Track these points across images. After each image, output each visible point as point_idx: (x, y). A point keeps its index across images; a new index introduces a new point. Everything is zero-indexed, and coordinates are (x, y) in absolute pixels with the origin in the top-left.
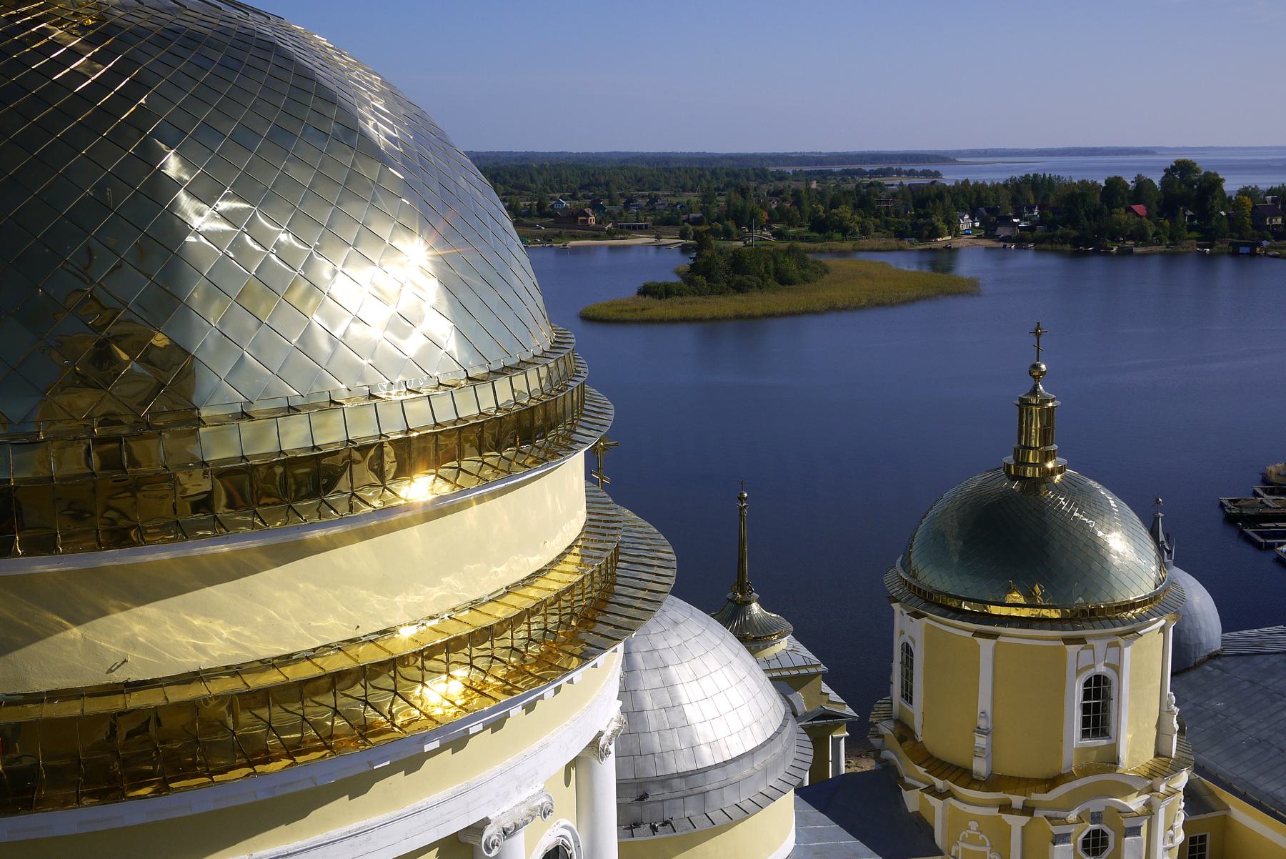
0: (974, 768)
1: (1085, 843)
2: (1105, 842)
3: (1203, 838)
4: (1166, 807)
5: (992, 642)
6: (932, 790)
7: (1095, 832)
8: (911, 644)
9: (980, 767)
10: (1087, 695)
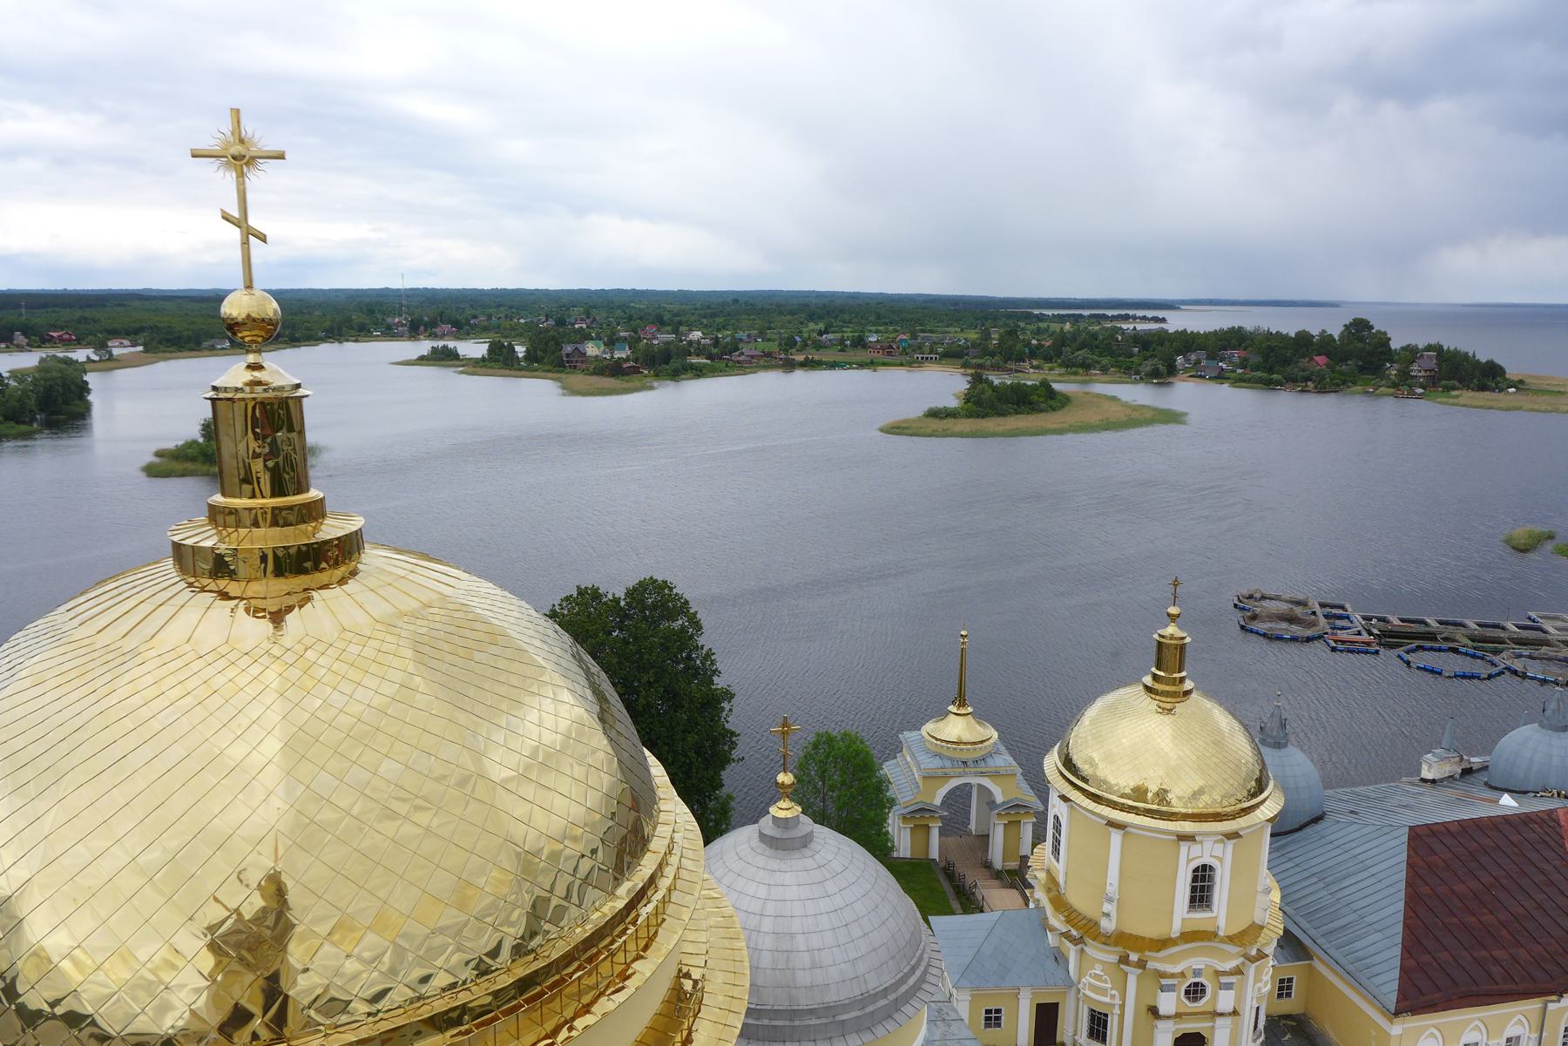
0: (1102, 924)
1: (1187, 992)
2: (1203, 991)
3: (1290, 980)
4: (1256, 967)
5: (1122, 832)
6: (1066, 935)
7: (1196, 984)
8: (1060, 818)
9: (1108, 925)
10: (1195, 879)
